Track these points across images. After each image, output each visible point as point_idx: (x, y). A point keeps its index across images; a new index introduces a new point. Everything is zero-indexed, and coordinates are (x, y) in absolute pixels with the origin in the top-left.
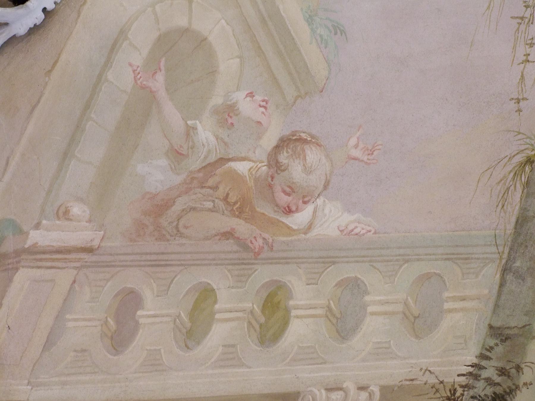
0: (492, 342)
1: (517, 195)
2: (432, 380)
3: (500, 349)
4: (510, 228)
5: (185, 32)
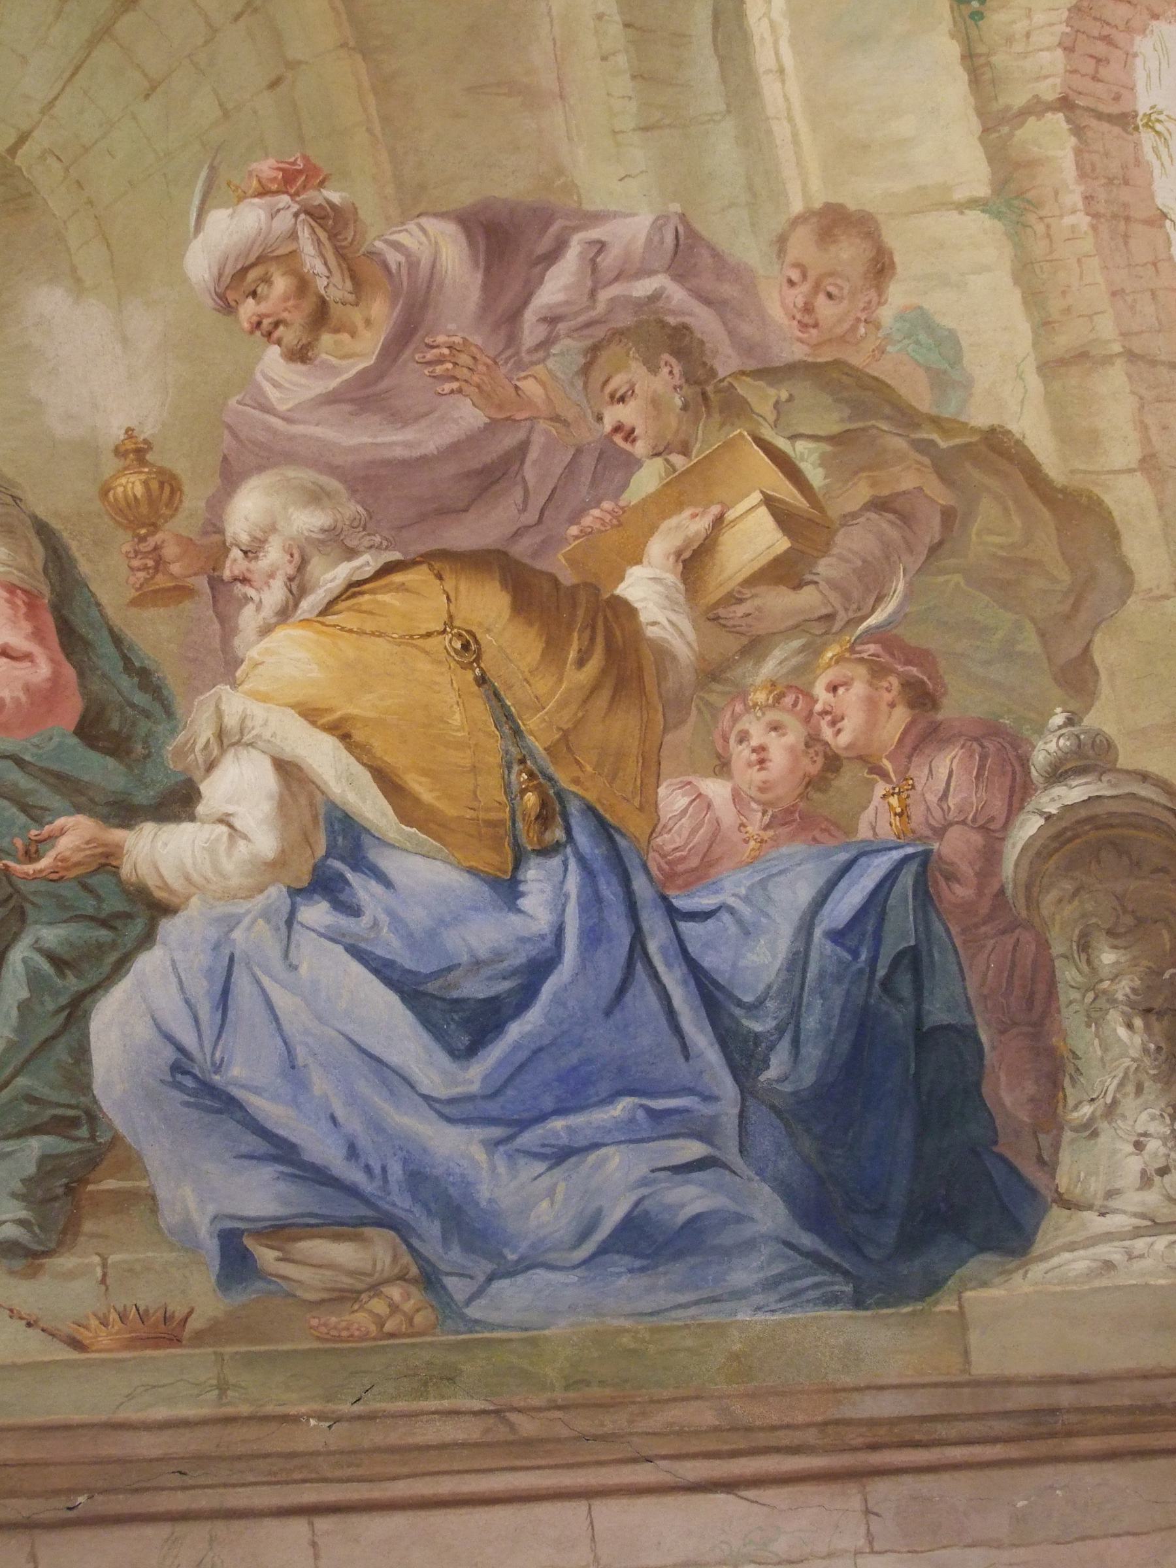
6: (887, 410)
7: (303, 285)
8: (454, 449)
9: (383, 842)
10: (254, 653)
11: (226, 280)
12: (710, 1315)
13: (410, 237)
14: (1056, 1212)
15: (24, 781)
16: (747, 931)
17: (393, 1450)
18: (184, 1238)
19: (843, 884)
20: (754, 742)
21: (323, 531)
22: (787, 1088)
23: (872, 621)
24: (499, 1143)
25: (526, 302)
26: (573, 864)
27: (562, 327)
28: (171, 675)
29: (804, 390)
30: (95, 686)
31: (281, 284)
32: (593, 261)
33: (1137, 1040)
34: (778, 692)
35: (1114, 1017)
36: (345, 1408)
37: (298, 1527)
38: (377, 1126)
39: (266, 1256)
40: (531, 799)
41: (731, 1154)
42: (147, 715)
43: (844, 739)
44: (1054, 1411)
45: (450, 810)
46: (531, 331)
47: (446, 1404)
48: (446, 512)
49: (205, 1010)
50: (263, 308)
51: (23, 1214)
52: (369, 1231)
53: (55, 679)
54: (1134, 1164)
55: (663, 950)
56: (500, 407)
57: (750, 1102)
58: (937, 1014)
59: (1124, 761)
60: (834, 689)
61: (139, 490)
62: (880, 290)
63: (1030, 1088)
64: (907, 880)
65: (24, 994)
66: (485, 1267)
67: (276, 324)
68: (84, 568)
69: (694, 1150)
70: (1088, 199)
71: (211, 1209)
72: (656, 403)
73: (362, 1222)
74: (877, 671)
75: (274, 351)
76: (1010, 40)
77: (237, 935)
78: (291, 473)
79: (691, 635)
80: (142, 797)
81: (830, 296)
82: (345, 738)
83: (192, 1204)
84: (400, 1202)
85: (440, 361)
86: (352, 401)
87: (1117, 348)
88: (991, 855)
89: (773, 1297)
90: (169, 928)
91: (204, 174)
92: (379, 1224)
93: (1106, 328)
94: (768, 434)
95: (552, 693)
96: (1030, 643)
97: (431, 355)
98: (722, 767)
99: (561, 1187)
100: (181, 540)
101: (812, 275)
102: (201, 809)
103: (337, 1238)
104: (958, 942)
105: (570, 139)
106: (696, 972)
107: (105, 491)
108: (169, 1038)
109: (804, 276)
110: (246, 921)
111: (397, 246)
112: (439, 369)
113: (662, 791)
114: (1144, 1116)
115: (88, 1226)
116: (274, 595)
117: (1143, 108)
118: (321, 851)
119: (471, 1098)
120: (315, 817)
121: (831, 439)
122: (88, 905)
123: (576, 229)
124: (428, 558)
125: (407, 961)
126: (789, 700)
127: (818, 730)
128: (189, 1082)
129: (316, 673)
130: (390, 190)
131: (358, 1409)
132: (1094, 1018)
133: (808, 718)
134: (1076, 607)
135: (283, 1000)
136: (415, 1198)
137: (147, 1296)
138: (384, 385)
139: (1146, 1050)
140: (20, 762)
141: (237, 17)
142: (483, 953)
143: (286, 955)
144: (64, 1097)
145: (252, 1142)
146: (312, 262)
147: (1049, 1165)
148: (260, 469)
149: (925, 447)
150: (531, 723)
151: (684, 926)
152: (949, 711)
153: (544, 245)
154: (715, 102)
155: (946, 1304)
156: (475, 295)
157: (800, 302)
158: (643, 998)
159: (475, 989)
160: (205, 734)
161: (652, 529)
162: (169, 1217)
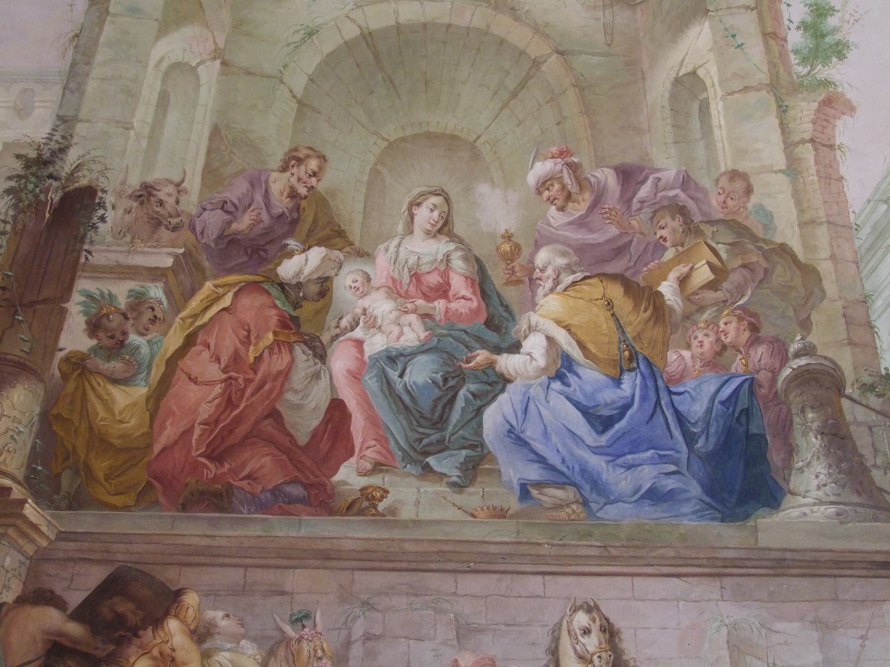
0: (58, 123)
1: (70, 52)
2: (29, 140)
3: (62, 127)
4: (67, 68)
6: (748, 236)
7: (564, 187)
8: (608, 242)
9: (578, 364)
10: (542, 302)
11: (540, 184)
13: (599, 174)
14: (789, 496)
15: (467, 338)
16: (693, 399)
17: (572, 556)
18: (509, 485)
19: (725, 386)
20: (699, 340)
21: (566, 265)
22: (703, 450)
23: (739, 303)
24: (610, 462)
25: (634, 196)
26: (639, 375)
27: (645, 204)
28: (515, 309)
29: (721, 228)
30: (491, 310)
31: (557, 186)
32: (656, 184)
33: (818, 442)
34: (708, 324)
35: (811, 435)
36: (556, 542)
37: (539, 578)
38: (572, 454)
39: (534, 492)
40: (627, 353)
41: (684, 470)
42: (507, 320)
43: (728, 340)
44: (785, 560)
45: (601, 355)
46: (635, 205)
47: (589, 543)
48: (605, 261)
49: (519, 414)
50: (551, 194)
51: (459, 474)
52: (567, 487)
53: (479, 307)
54: (815, 482)
55: (666, 404)
56: (624, 229)
57: (692, 454)
58: (754, 430)
59: (819, 353)
60: (726, 324)
61: (508, 249)
62: (748, 198)
63: (782, 455)
64: (746, 386)
65: (463, 405)
66: (604, 500)
67: (555, 199)
68: (490, 272)
69: (673, 468)
70: (818, 171)
71: (518, 476)
72: (674, 230)
73: (564, 484)
74: (740, 319)
75: (553, 207)
76: (795, 120)
77: (531, 391)
78: (556, 246)
79: (681, 304)
80: (504, 345)
81: (732, 199)
82: (569, 331)
83: (512, 474)
84: (578, 479)
85: (606, 213)
86: (577, 224)
87: (824, 220)
88: (774, 380)
89: (695, 517)
90: (510, 387)
91: (534, 151)
92: (570, 484)
93: (822, 213)
94: (709, 241)
95: (636, 320)
96: (791, 313)
97: (603, 211)
98: (688, 347)
99: (629, 477)
100: (520, 264)
101: (726, 192)
102: (522, 350)
103: (557, 488)
104: (762, 407)
105: (651, 145)
107: (497, 249)
108: (508, 422)
109: (724, 192)
110: (535, 386)
111: (594, 176)
112: (605, 216)
113: (669, 353)
114: (819, 467)
115: (479, 479)
116: (549, 284)
117: (837, 143)
118: (559, 366)
119: (602, 447)
120: (558, 355)
121: (729, 244)
122: (485, 378)
123: (651, 174)
124: (598, 275)
125: (584, 401)
126: (711, 327)
127: (720, 337)
128: (513, 436)
129: (561, 310)
130: (593, 159)
131: (560, 542)
132: (805, 434)
133: (717, 333)
134: (806, 302)
135: (544, 412)
136: (582, 477)
137: (496, 502)
138: (586, 220)
139: (821, 446)
140: (466, 332)
141: (548, 102)
142: (608, 401)
143: (546, 398)
144: (474, 438)
145: (532, 456)
146: (567, 180)
147: (787, 480)
148: (547, 244)
149: (760, 248)
150: (628, 330)
151: (673, 397)
152: (762, 333)
153: (641, 178)
154: (697, 135)
155: (751, 523)
156: (618, 193)
157: (722, 200)
158: (659, 418)
159: (606, 412)
160: (525, 327)
161: (670, 270)
162: (505, 478)
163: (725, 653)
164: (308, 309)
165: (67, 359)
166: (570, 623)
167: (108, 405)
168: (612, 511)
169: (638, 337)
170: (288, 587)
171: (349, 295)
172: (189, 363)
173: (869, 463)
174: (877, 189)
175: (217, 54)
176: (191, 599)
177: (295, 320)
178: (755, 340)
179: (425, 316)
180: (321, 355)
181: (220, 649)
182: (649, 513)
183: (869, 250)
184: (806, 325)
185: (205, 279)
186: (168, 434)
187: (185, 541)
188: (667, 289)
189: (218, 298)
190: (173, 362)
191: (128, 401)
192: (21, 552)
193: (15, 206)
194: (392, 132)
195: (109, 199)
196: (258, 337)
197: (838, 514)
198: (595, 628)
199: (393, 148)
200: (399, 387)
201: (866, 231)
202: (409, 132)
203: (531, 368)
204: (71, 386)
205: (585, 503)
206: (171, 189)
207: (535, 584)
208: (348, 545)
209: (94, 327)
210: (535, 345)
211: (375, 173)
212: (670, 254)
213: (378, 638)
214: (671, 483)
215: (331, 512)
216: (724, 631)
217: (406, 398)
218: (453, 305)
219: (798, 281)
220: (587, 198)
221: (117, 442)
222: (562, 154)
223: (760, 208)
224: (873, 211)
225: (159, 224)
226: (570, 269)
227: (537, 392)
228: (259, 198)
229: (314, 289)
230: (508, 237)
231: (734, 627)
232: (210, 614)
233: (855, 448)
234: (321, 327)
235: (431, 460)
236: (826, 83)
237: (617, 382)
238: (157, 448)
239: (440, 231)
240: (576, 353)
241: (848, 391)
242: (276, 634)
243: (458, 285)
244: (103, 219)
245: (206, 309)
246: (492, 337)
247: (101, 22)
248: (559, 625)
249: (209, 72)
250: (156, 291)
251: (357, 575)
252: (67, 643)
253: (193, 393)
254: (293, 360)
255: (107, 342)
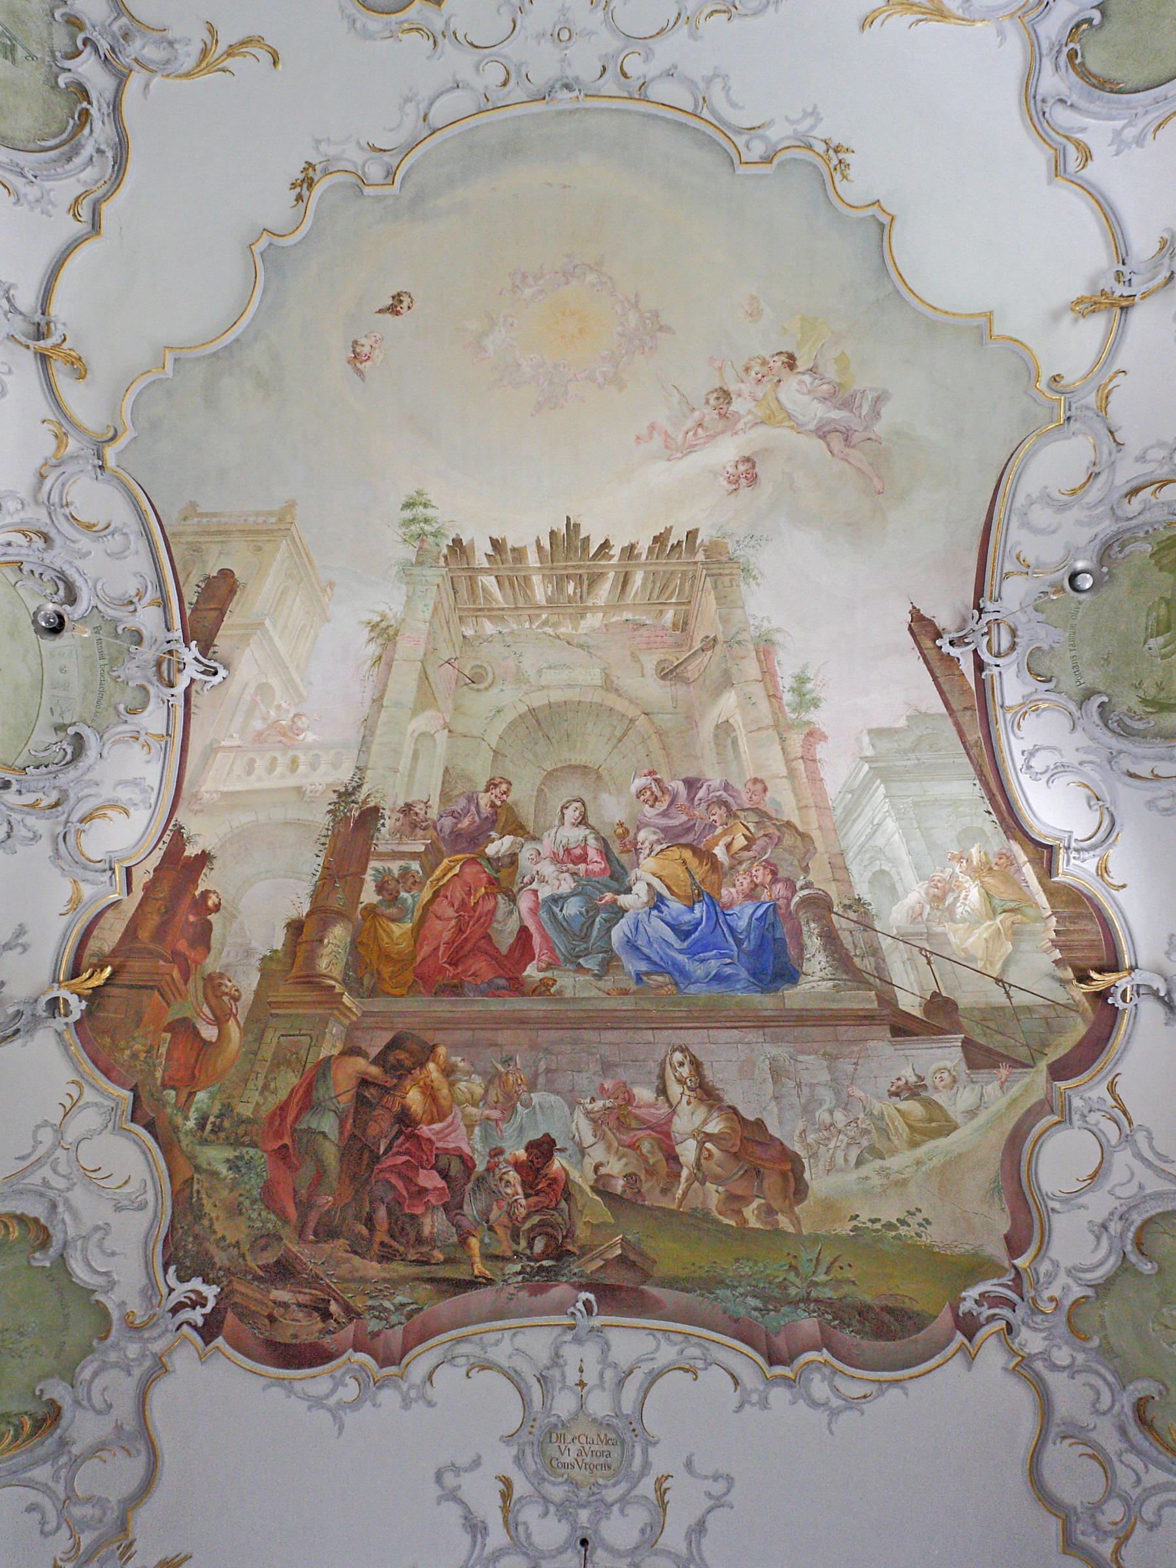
5: (265, 684)
7: (652, 793)
8: (681, 825)
12: (732, 994)
13: (673, 784)
29: (750, 813)
31: (649, 793)
38: (667, 954)
39: (645, 978)
41: (736, 961)
46: (696, 802)
48: (679, 836)
58: (778, 936)
66: (687, 983)
69: (729, 961)
72: (721, 816)
74: (765, 868)
84: (671, 969)
88: (788, 905)
93: (811, 801)
96: (796, 863)
98: (734, 886)
106: (729, 926)
116: (647, 851)
132: (810, 937)
137: (622, 985)
146: (654, 789)
159: (685, 928)
163: (769, 1076)
164: (504, 872)
165: (365, 908)
166: (671, 1058)
167: (389, 934)
168: (693, 989)
169: (703, 881)
170: (499, 1040)
171: (528, 863)
172: (434, 907)
173: (852, 954)
174: (844, 785)
175: (446, 726)
176: (441, 1050)
177: (497, 879)
178: (775, 881)
179: (573, 874)
180: (513, 899)
181: (460, 1080)
182: (716, 988)
183: (843, 821)
184: (806, 870)
185: (444, 858)
186: (426, 950)
187: (438, 1015)
188: (719, 851)
189: (452, 868)
190: (426, 907)
191: (401, 931)
192: (341, 1023)
193: (334, 820)
194: (549, 766)
195: (387, 813)
196: (476, 891)
197: (834, 986)
198: (687, 1062)
199: (550, 775)
200: (560, 917)
201: (839, 810)
202: (559, 766)
203: (639, 903)
204: (368, 924)
205: (676, 984)
206: (422, 806)
207: (649, 1035)
208: (534, 1014)
209: (380, 888)
210: (640, 889)
211: (540, 791)
212: (719, 830)
213: (556, 1071)
214: (728, 970)
215: (523, 995)
216: (767, 1062)
217: (565, 924)
218: (590, 867)
219: (799, 843)
220: (667, 798)
221: (395, 956)
222: (650, 773)
223: (773, 800)
224: (843, 798)
225: (416, 826)
226: (659, 842)
227: (643, 917)
228: (473, 808)
229: (507, 860)
230: (621, 824)
231: (773, 1060)
232: (453, 1059)
233: (842, 944)
234: (512, 883)
235: (581, 961)
236: (809, 723)
237: (692, 909)
238: (419, 959)
239: (580, 823)
240: (665, 892)
241: (835, 909)
242: (493, 1070)
243: (593, 854)
244: (383, 825)
245: (445, 875)
246: (614, 884)
247: (379, 712)
248: (665, 1060)
249: (442, 737)
250: (415, 866)
251: (540, 1032)
252: (370, 1079)
253: (439, 925)
254: (496, 903)
255: (389, 897)
